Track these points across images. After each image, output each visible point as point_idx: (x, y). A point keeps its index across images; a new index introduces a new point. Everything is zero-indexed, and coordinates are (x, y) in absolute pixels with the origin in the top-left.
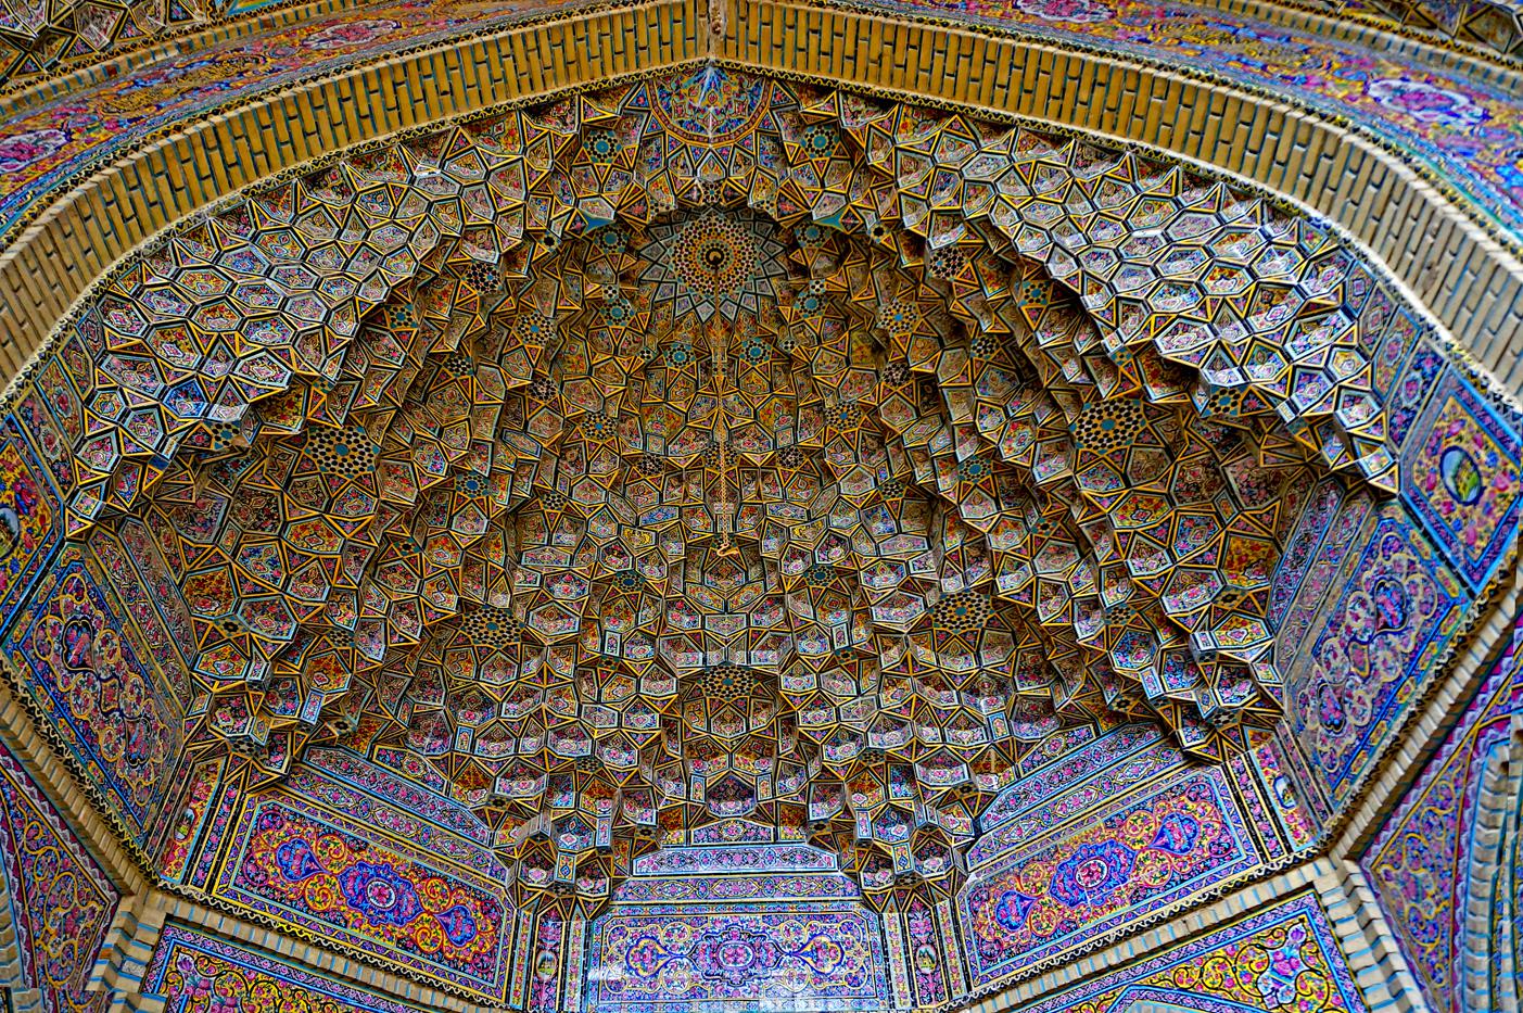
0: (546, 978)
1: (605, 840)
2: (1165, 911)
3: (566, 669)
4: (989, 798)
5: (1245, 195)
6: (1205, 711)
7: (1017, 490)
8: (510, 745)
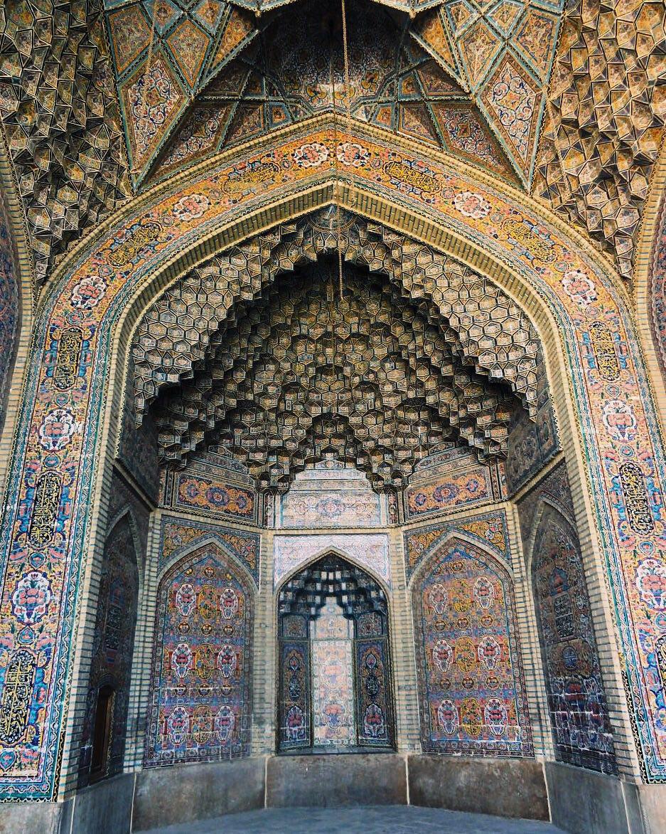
0: (268, 514)
1: (287, 472)
2: (464, 508)
3: (273, 416)
4: (418, 460)
5: (518, 307)
6: (485, 453)
7: (436, 371)
8: (254, 442)
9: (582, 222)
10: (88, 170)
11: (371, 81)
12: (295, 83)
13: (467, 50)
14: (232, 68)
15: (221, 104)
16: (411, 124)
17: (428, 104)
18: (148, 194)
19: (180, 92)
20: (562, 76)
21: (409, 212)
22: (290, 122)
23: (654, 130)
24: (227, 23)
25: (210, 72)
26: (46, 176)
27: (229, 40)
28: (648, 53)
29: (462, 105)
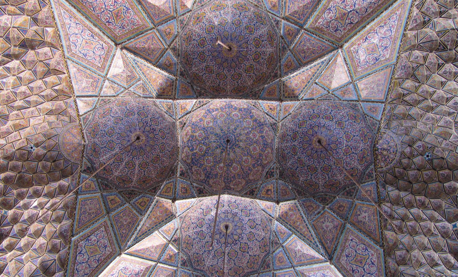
12: (258, 15)
13: (132, 72)
15: (317, 31)
17: (151, 26)
20: (59, 64)
24: (304, 88)
27: (304, 78)
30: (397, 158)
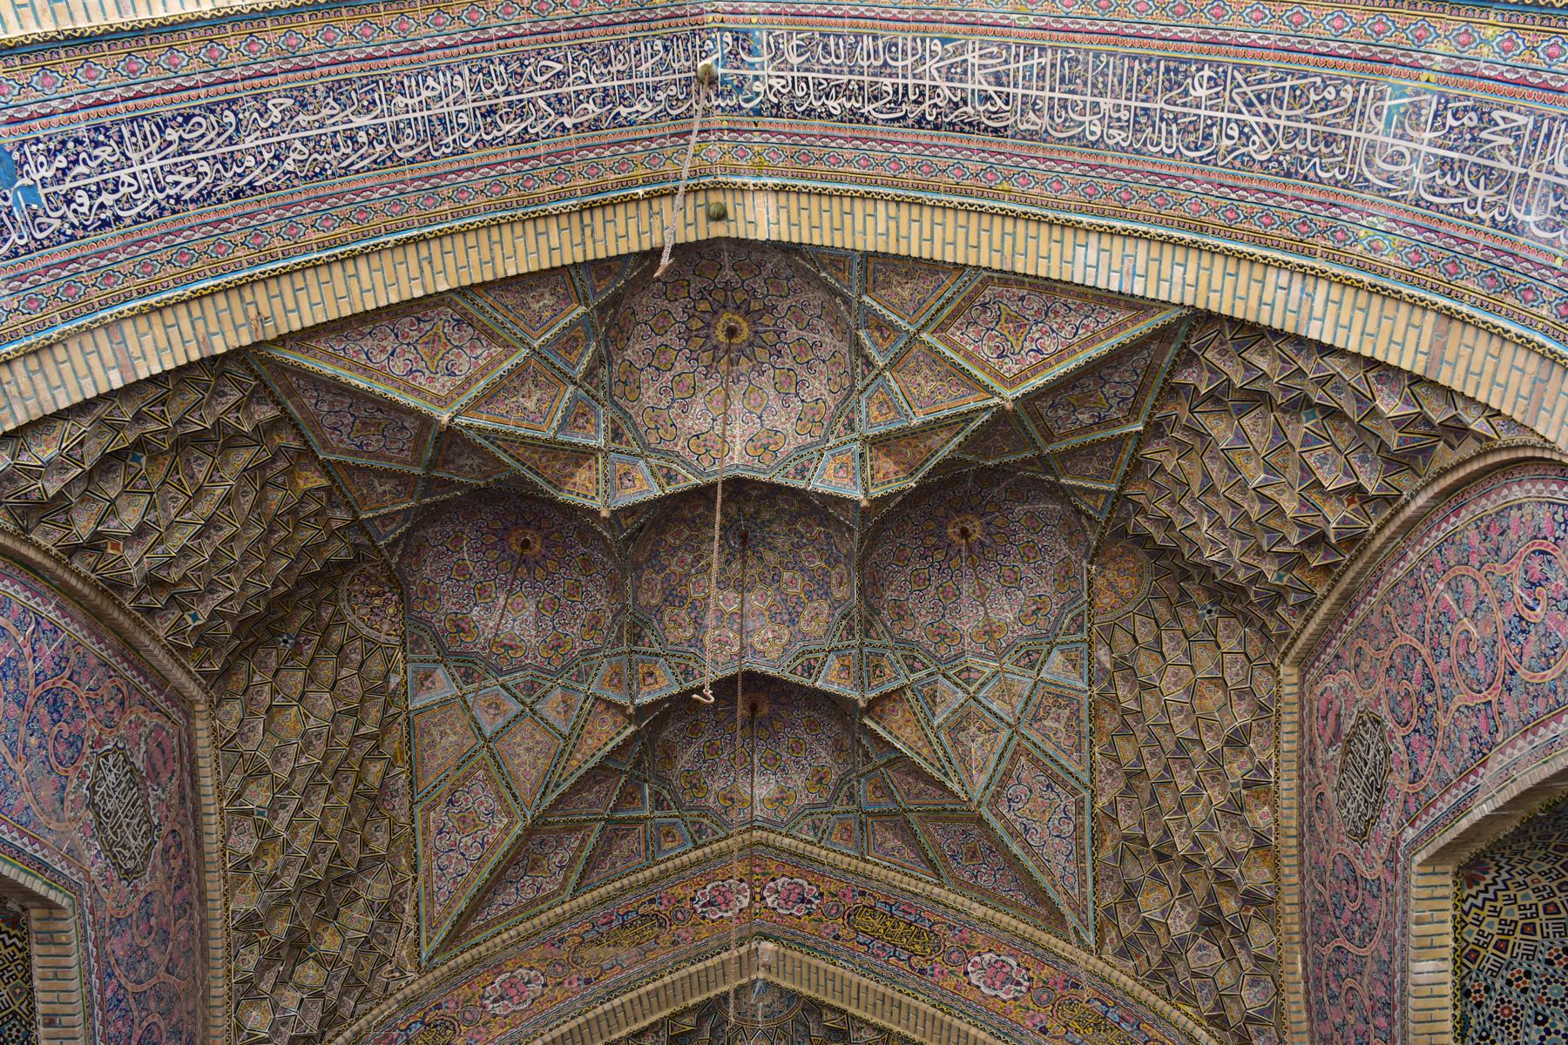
9: (1187, 997)
10: (350, 934)
11: (820, 781)
12: (699, 789)
13: (956, 742)
14: (599, 773)
16: (889, 845)
17: (911, 817)
18: (445, 969)
19: (509, 814)
20: (1110, 772)
21: (889, 991)
22: (690, 846)
23: (1261, 852)
25: (557, 785)
26: (279, 948)
28: (1219, 745)
29: (959, 817)
30: (343, 588)
